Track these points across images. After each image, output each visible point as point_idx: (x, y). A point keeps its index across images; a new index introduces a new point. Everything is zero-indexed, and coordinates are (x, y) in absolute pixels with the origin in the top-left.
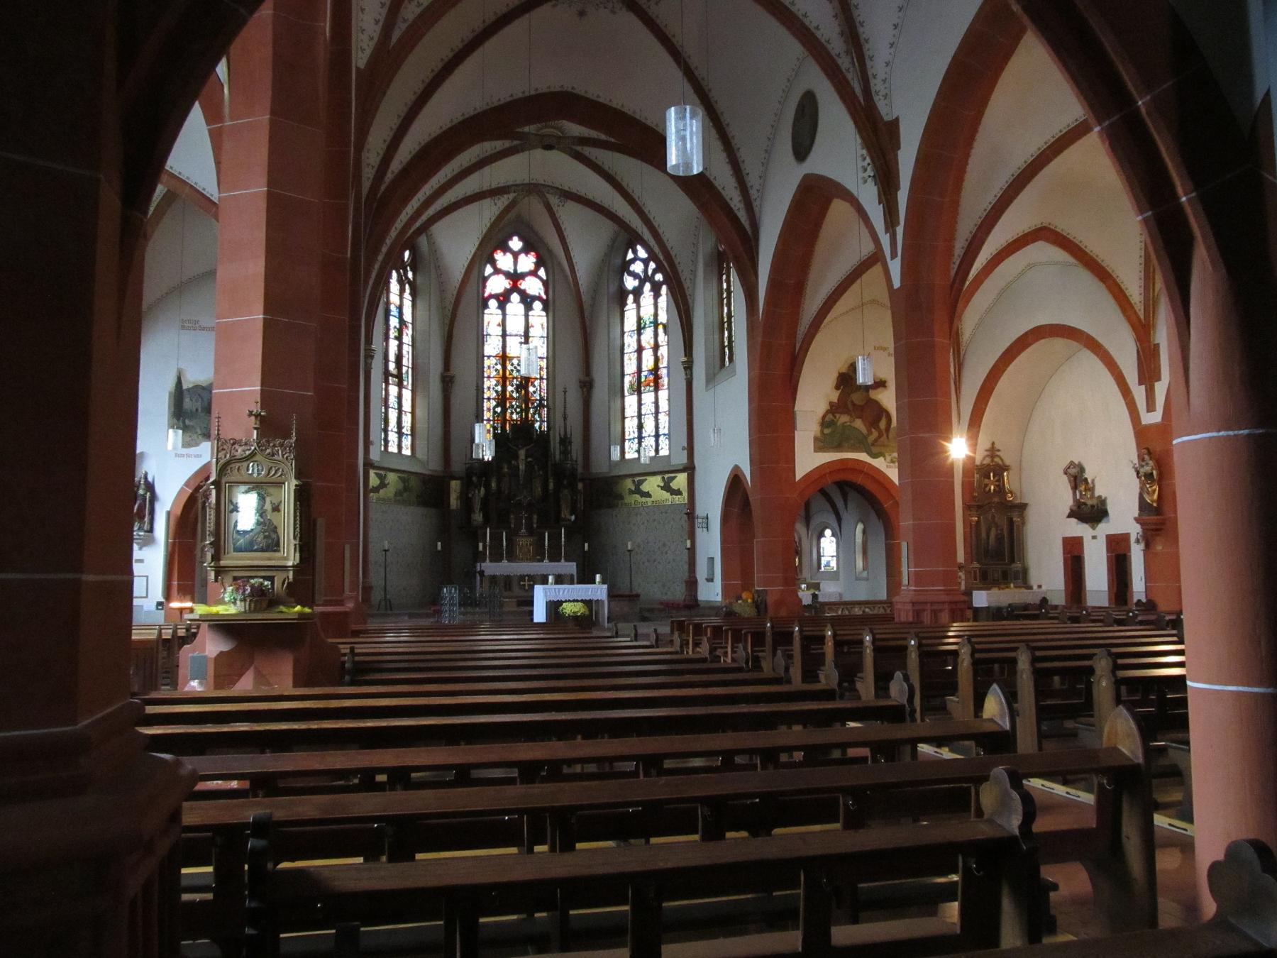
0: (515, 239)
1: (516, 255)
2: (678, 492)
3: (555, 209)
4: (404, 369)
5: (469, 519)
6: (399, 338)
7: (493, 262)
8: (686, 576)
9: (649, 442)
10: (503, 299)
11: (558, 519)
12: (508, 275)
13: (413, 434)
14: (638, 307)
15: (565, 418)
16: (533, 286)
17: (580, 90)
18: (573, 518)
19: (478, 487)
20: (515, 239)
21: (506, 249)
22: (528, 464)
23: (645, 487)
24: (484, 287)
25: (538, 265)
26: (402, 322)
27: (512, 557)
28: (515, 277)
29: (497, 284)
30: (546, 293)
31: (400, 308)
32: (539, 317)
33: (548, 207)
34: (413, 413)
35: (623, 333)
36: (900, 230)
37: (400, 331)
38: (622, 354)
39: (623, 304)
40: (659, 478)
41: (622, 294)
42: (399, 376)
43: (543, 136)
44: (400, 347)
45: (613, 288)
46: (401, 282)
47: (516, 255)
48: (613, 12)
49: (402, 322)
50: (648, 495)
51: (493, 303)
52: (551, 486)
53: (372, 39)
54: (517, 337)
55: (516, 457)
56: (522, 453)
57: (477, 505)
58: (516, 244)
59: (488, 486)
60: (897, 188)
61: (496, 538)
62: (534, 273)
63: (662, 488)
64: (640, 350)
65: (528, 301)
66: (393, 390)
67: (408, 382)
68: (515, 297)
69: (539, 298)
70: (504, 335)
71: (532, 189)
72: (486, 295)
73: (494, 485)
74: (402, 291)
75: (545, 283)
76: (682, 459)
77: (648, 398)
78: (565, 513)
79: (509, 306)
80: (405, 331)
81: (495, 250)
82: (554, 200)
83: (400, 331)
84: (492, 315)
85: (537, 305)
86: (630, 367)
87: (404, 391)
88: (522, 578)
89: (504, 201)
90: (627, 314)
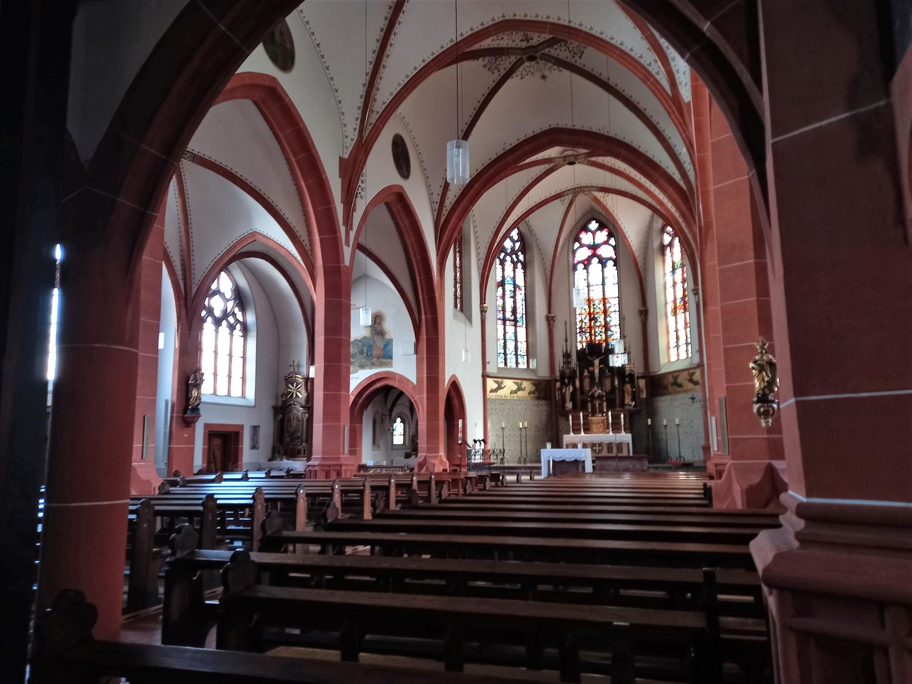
1: (594, 233)
2: (696, 383)
3: (602, 200)
4: (519, 316)
5: (564, 407)
6: (514, 297)
7: (577, 239)
8: (702, 442)
9: (683, 348)
10: (587, 263)
11: (623, 405)
12: (590, 247)
14: (672, 254)
17: (562, 125)
18: (633, 404)
19: (568, 385)
21: (585, 229)
22: (600, 369)
23: (679, 381)
24: (574, 257)
25: (610, 235)
26: (515, 286)
27: (587, 430)
28: (594, 247)
29: (582, 254)
31: (514, 278)
33: (596, 200)
34: (527, 341)
35: (665, 274)
37: (514, 292)
38: (665, 288)
39: (663, 254)
40: (686, 373)
41: (663, 248)
42: (515, 321)
43: (565, 157)
44: (515, 302)
45: (656, 244)
46: (512, 261)
47: (594, 233)
49: (515, 286)
50: (680, 386)
51: (581, 266)
52: (616, 383)
54: (595, 285)
55: (593, 365)
56: (597, 362)
57: (568, 398)
58: (594, 225)
59: (574, 385)
62: (606, 243)
64: (675, 284)
65: (603, 262)
66: (510, 329)
67: (522, 323)
68: (595, 260)
69: (611, 259)
71: (576, 191)
72: (576, 261)
73: (577, 383)
74: (515, 268)
75: (615, 248)
76: (696, 360)
77: (681, 316)
78: (628, 400)
79: (591, 268)
80: (518, 292)
81: (580, 232)
82: (599, 195)
83: (514, 292)
84: (580, 273)
86: (670, 298)
87: (518, 329)
89: (567, 199)
90: (667, 261)
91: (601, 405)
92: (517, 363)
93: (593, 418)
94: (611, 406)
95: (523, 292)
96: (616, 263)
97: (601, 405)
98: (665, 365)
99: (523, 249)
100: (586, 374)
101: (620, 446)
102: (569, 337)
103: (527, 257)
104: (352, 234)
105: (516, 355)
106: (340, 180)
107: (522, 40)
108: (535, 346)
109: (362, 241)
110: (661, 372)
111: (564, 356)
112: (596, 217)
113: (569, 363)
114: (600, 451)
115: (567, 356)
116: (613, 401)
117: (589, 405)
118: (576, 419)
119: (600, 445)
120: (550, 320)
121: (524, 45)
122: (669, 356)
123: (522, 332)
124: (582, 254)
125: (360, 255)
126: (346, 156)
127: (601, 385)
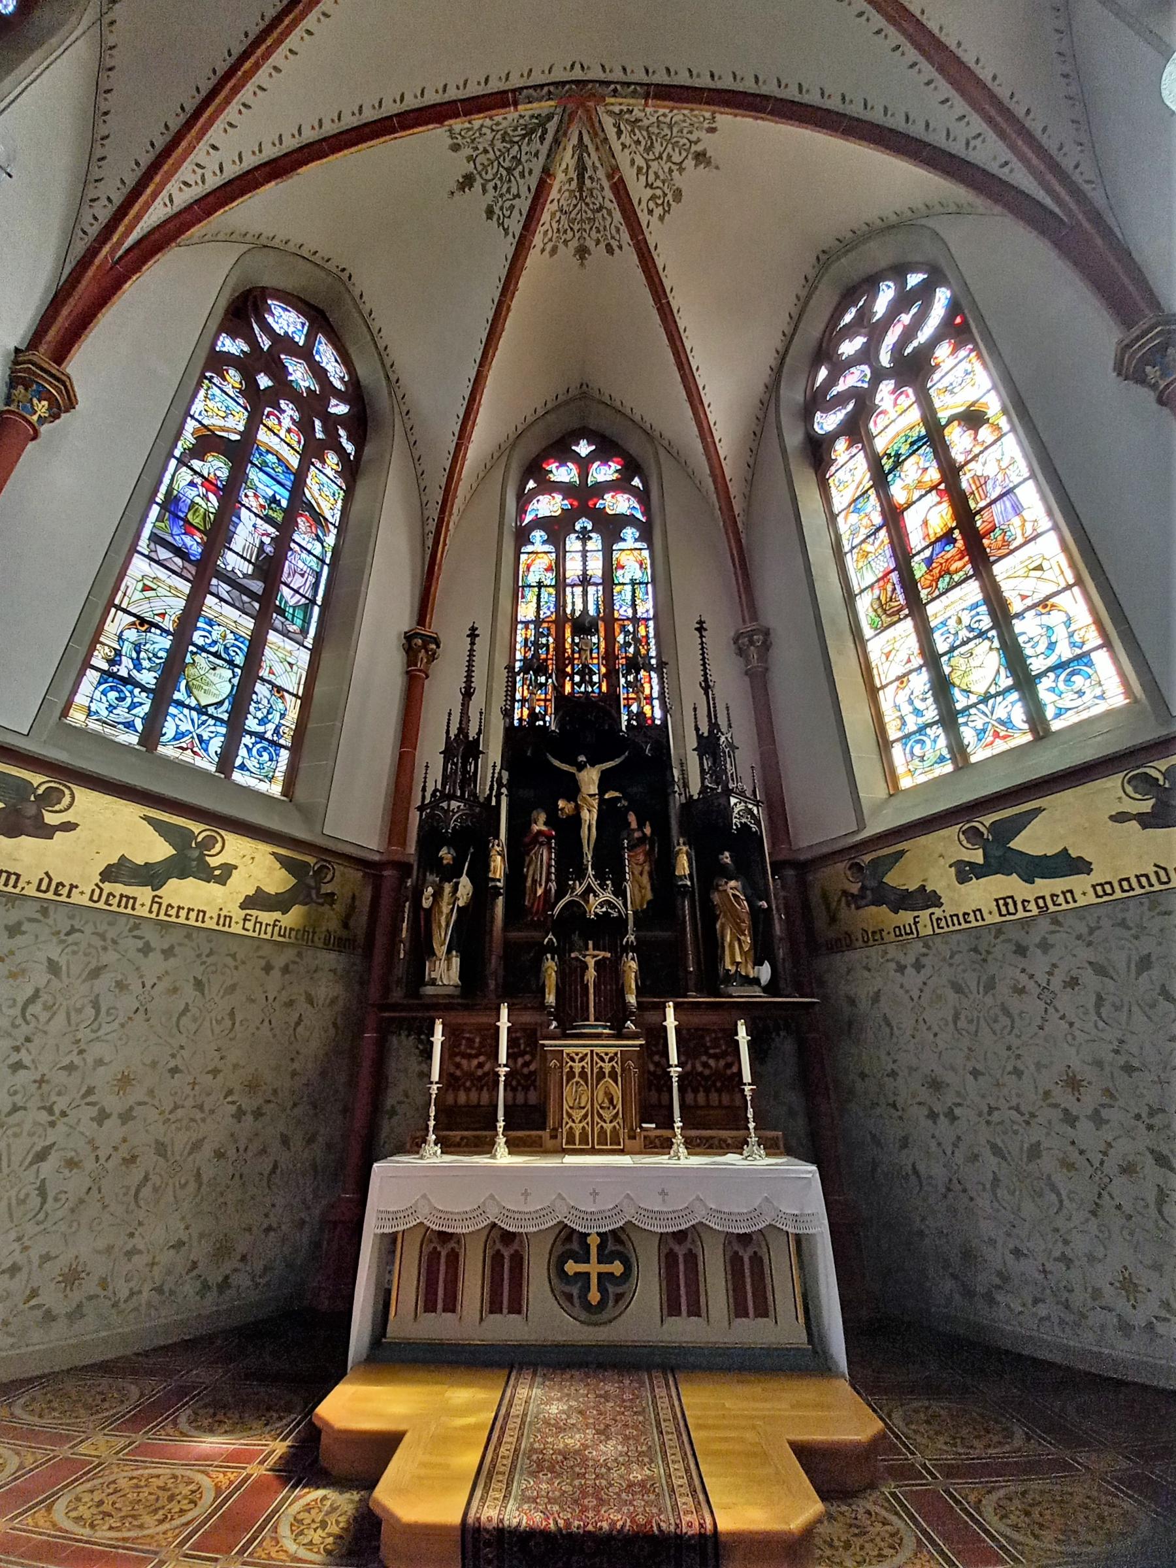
0: (583, 443)
1: (584, 465)
3: (643, 217)
5: (417, 977)
11: (712, 977)
13: (296, 749)
15: (706, 688)
16: (620, 504)
18: (765, 973)
19: (451, 874)
20: (583, 443)
21: (563, 453)
22: (607, 812)
24: (522, 511)
25: (631, 467)
27: (532, 1124)
30: (647, 511)
32: (632, 557)
34: (306, 700)
41: (818, 453)
45: (794, 438)
47: (584, 465)
51: (538, 535)
52: (683, 866)
59: (480, 875)
61: (472, 1044)
63: (1146, 821)
65: (611, 527)
70: (560, 584)
73: (498, 866)
78: (736, 952)
79: (573, 544)
84: (537, 561)
85: (629, 533)
88: (569, 1242)
91: (610, 971)
92: (226, 761)
93: (571, 1047)
94: (660, 982)
95: (331, 540)
96: (646, 535)
97: (610, 971)
98: (880, 806)
99: (361, 423)
100: (539, 826)
101: (748, 1256)
102: (479, 682)
103: (368, 450)
105: (235, 727)
108: (336, 710)
110: (874, 828)
111: (448, 753)
112: (593, 424)
113: (469, 780)
114: (616, 1289)
115: (462, 749)
116: (675, 955)
117: (550, 966)
118: (472, 1044)
119: (616, 1243)
120: (419, 648)
122: (890, 775)
123: (286, 660)
124: (548, 506)
127: (610, 867)
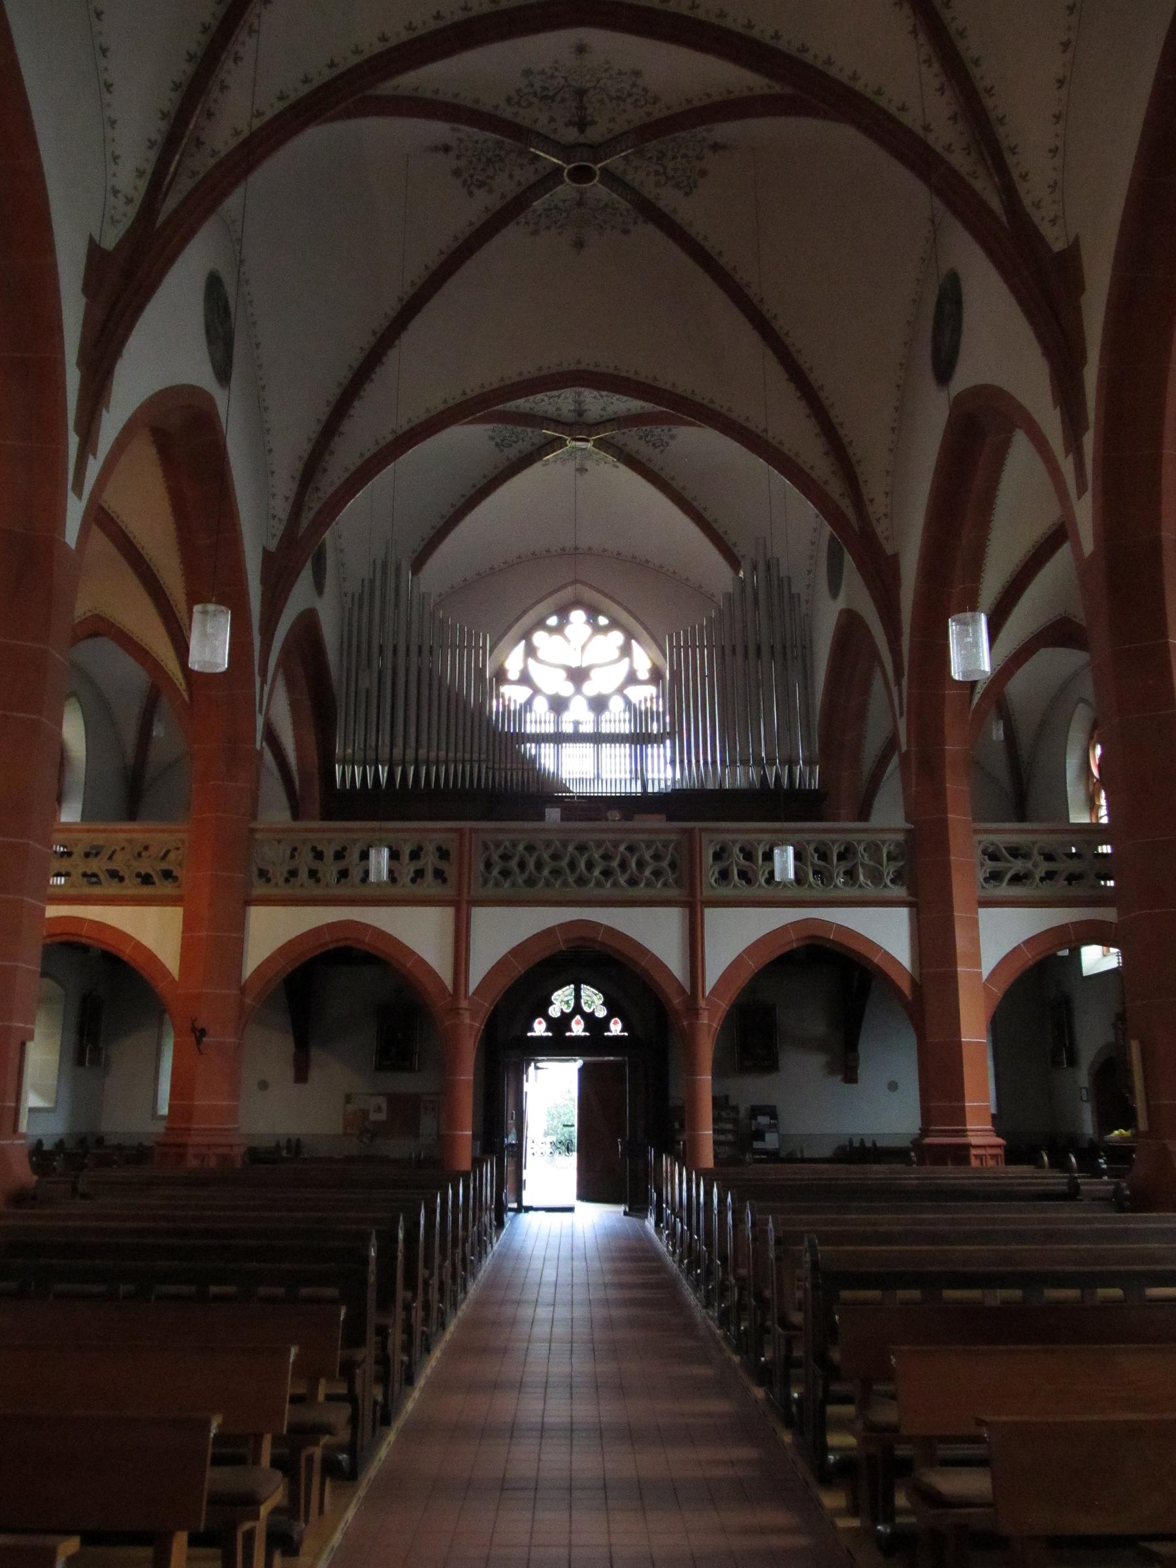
36: (1089, 441)
48: (626, 232)
53: (129, 201)
60: (1082, 359)
104: (94, 468)
106: (82, 301)
107: (569, 123)
109: (114, 502)
121: (571, 135)
125: (100, 541)
126: (109, 242)
